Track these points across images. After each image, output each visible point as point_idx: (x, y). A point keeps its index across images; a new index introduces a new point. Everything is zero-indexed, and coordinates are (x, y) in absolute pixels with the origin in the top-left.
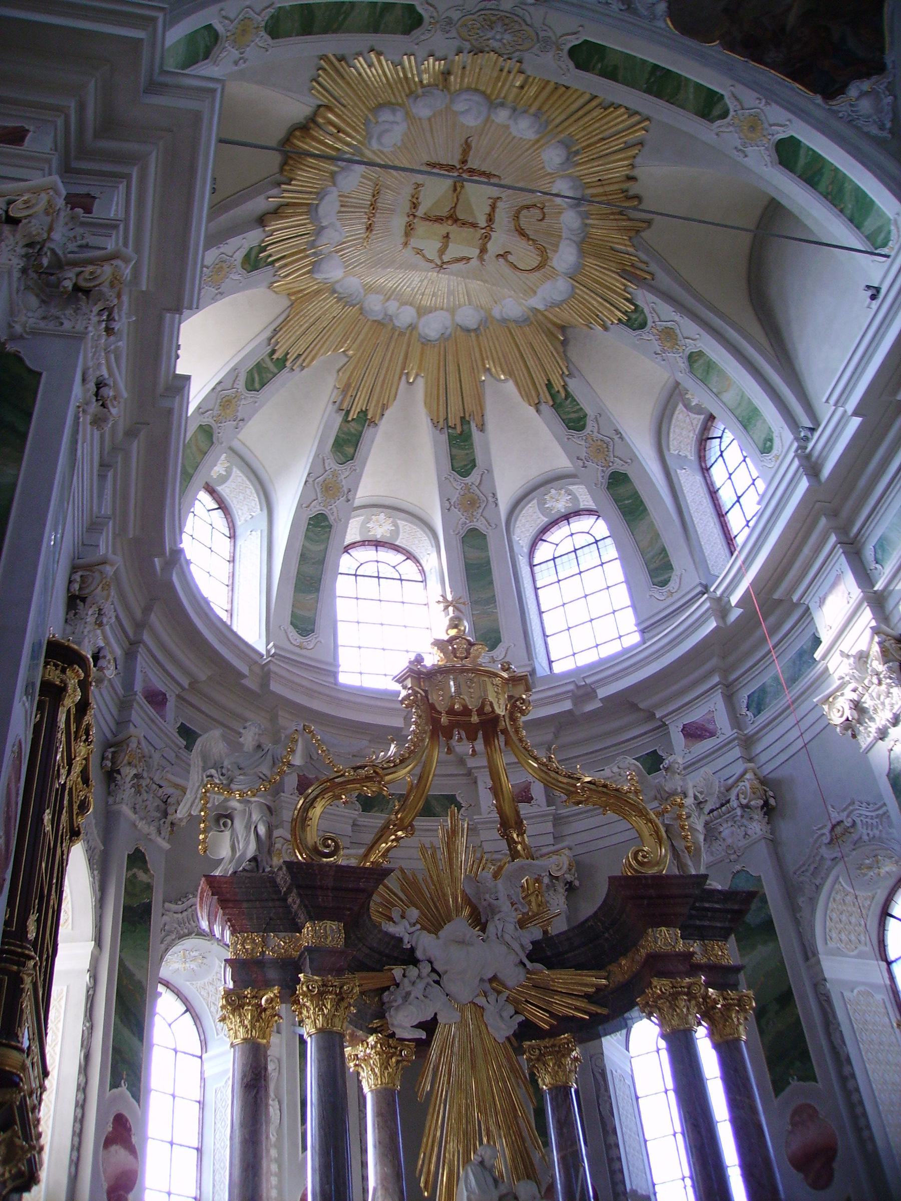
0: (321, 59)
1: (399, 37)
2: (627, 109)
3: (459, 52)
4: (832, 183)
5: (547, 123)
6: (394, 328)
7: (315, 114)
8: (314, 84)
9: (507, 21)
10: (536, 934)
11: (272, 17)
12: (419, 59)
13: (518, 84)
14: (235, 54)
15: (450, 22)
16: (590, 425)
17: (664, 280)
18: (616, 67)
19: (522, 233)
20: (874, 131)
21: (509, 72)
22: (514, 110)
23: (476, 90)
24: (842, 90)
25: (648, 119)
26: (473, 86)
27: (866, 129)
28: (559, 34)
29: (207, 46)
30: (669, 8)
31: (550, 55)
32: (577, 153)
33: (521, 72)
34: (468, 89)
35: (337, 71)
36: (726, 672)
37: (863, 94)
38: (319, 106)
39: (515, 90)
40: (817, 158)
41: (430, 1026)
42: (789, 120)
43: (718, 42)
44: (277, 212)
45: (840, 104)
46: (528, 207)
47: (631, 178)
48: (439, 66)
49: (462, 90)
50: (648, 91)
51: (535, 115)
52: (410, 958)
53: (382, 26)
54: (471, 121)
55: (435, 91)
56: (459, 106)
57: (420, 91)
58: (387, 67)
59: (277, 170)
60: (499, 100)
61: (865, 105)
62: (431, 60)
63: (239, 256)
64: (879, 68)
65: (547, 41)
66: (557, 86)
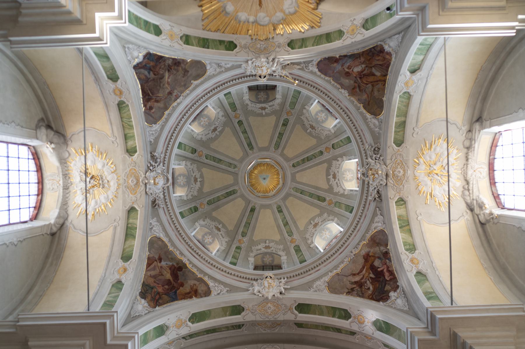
0: (320, 26)
1: (293, 39)
2: (212, 31)
3: (273, 38)
4: (140, 23)
5: (236, 20)
7: (317, 6)
8: (321, 17)
9: (260, 51)
11: (342, 37)
12: (286, 32)
13: (250, 31)
14: (355, 22)
15: (279, 47)
18: (220, 44)
20: (130, 46)
21: (254, 35)
22: (248, 22)
23: (263, 26)
24: (145, 57)
25: (204, 29)
26: (265, 27)
27: (133, 46)
28: (242, 51)
29: (367, 23)
30: (206, 68)
31: (243, 44)
32: (223, 11)
33: (250, 36)
34: (266, 25)
35: (313, 23)
37: (137, 57)
38: (317, 9)
39: (250, 28)
40: (148, 31)
42: (162, 42)
43: (188, 61)
45: (144, 52)
47: (201, 6)
48: (278, 31)
49: (268, 24)
50: (207, 39)
51: (240, 21)
53: (301, 41)
54: (261, 15)
55: (276, 22)
56: (267, 19)
57: (282, 22)
58: (296, 28)
60: (254, 24)
61: (136, 54)
62: (282, 33)
64: (135, 67)
65: (245, 48)
66: (236, 33)
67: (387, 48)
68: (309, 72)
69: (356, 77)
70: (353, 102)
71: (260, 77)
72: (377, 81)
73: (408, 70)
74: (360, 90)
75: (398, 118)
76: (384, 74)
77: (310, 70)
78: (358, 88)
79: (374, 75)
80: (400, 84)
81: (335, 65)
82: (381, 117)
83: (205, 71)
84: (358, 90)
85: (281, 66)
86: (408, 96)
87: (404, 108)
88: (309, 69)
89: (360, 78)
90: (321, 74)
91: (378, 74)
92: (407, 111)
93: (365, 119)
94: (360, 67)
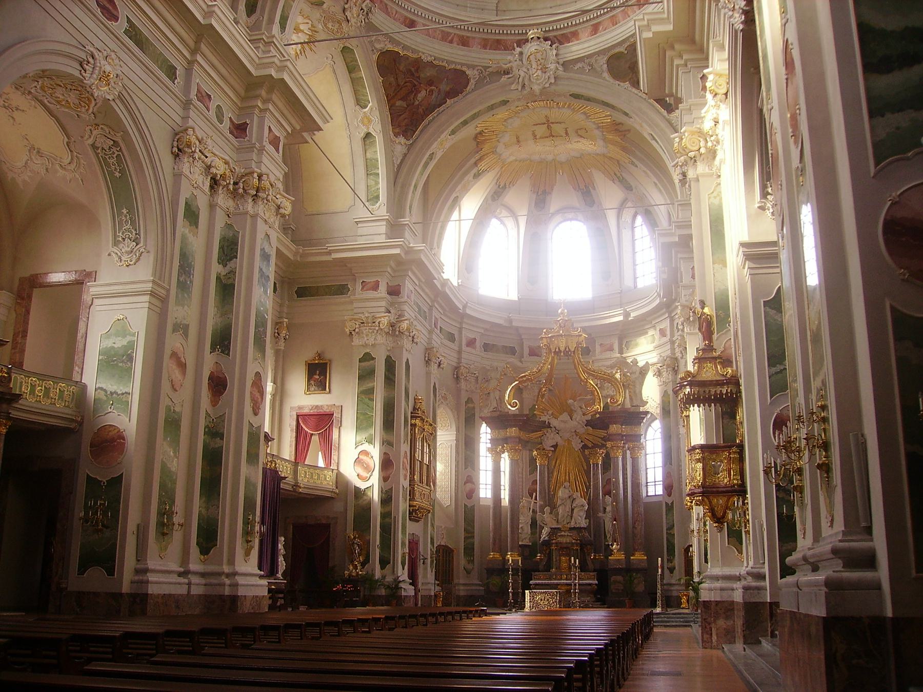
6: (547, 162)
10: (589, 417)
16: (634, 190)
17: (638, 153)
19: (581, 137)
32: (590, 116)
36: (670, 313)
41: (555, 446)
44: (481, 159)
46: (580, 129)
51: (569, 107)
52: (549, 426)
59: (475, 146)
63: (471, 178)
67: (402, 140)
68: (477, 66)
69: (420, 84)
70: (414, 51)
71: (539, 38)
72: (396, 94)
73: (375, 137)
74: (410, 70)
75: (360, 76)
76: (393, 108)
77: (477, 68)
78: (413, 71)
79: (401, 99)
80: (377, 120)
81: (448, 89)
82: (375, 57)
83: (608, 62)
84: (413, 69)
85: (513, 73)
86: (360, 103)
87: (359, 88)
88: (477, 70)
89: (415, 85)
90: (462, 69)
91: (399, 103)
92: (353, 85)
93: (392, 41)
94: (420, 99)
